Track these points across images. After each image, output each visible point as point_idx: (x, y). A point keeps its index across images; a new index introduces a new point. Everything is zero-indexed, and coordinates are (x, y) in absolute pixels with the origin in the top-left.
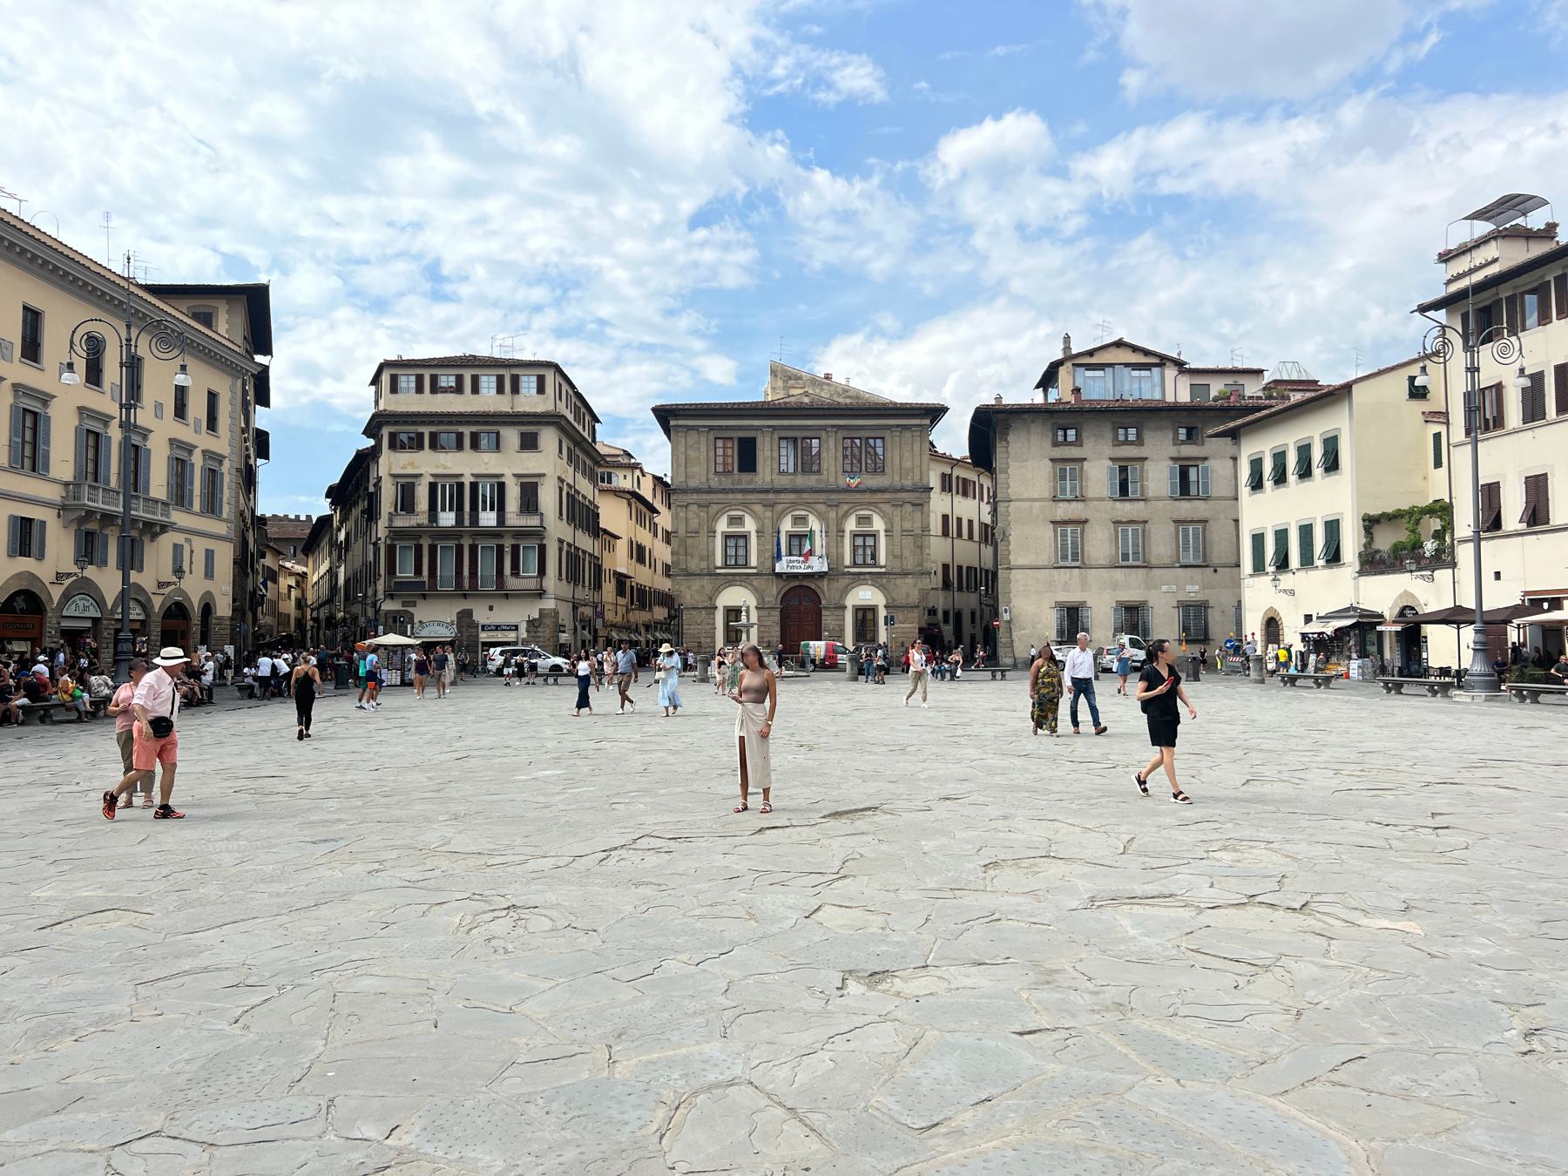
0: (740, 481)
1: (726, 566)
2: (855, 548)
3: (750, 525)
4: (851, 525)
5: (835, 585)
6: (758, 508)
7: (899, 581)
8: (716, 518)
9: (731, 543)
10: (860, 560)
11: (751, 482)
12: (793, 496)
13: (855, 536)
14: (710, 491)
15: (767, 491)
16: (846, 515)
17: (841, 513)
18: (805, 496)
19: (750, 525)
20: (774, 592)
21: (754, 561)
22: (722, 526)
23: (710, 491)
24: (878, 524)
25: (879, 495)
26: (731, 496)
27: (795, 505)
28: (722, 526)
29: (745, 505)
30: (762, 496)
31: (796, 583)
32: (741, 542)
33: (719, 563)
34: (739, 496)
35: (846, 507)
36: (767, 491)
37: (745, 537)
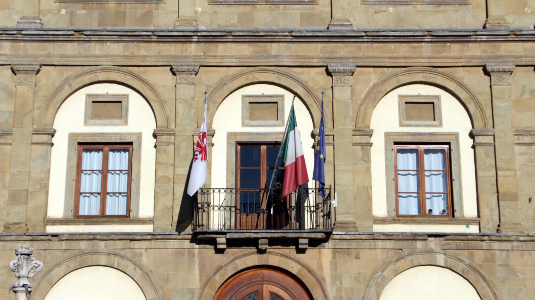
0: (121, 16)
1: (77, 218)
2: (394, 173)
3: (139, 120)
4: (386, 117)
5: (351, 267)
6: (162, 79)
7: (516, 260)
8: (56, 99)
9: (92, 160)
10: (410, 207)
11: (148, 16)
12: (245, 50)
13: (401, 145)
14: (46, 37)
15: (184, 38)
16: (374, 96)
17: (363, 90)
18: (274, 48)
19: (139, 120)
20: (196, 283)
21: (146, 207)
22: (72, 118)
23: (46, 37)
24: (454, 119)
25: (455, 49)
26: (96, 49)
27: (250, 71)
28: (72, 118)
29: (128, 73)
30: (171, 50)
31: (254, 259)
32: (119, 160)
33: (57, 208)
34: (116, 49)
35: (373, 77)
36: (184, 38)
37: (125, 146)
